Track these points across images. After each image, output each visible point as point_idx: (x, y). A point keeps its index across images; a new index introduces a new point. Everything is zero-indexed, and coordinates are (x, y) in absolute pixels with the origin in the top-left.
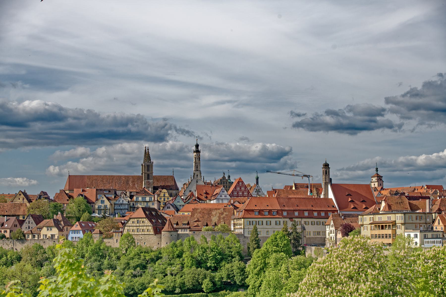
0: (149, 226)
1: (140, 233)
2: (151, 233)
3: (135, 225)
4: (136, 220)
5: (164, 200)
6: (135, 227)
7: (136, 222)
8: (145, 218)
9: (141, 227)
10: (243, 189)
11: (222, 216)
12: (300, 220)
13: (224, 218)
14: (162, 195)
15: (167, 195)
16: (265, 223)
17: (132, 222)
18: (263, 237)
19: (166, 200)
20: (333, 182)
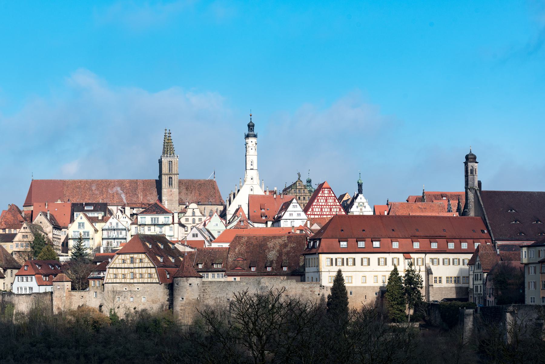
0: (151, 268)
1: (135, 281)
2: (154, 281)
3: (126, 266)
4: (128, 256)
5: (194, 221)
6: (126, 270)
7: (129, 261)
8: (144, 253)
9: (137, 270)
10: (330, 201)
11: (285, 250)
12: (423, 256)
13: (288, 253)
14: (189, 212)
15: (197, 212)
16: (358, 262)
17: (121, 261)
18: (355, 287)
19: (197, 221)
20: (483, 189)
